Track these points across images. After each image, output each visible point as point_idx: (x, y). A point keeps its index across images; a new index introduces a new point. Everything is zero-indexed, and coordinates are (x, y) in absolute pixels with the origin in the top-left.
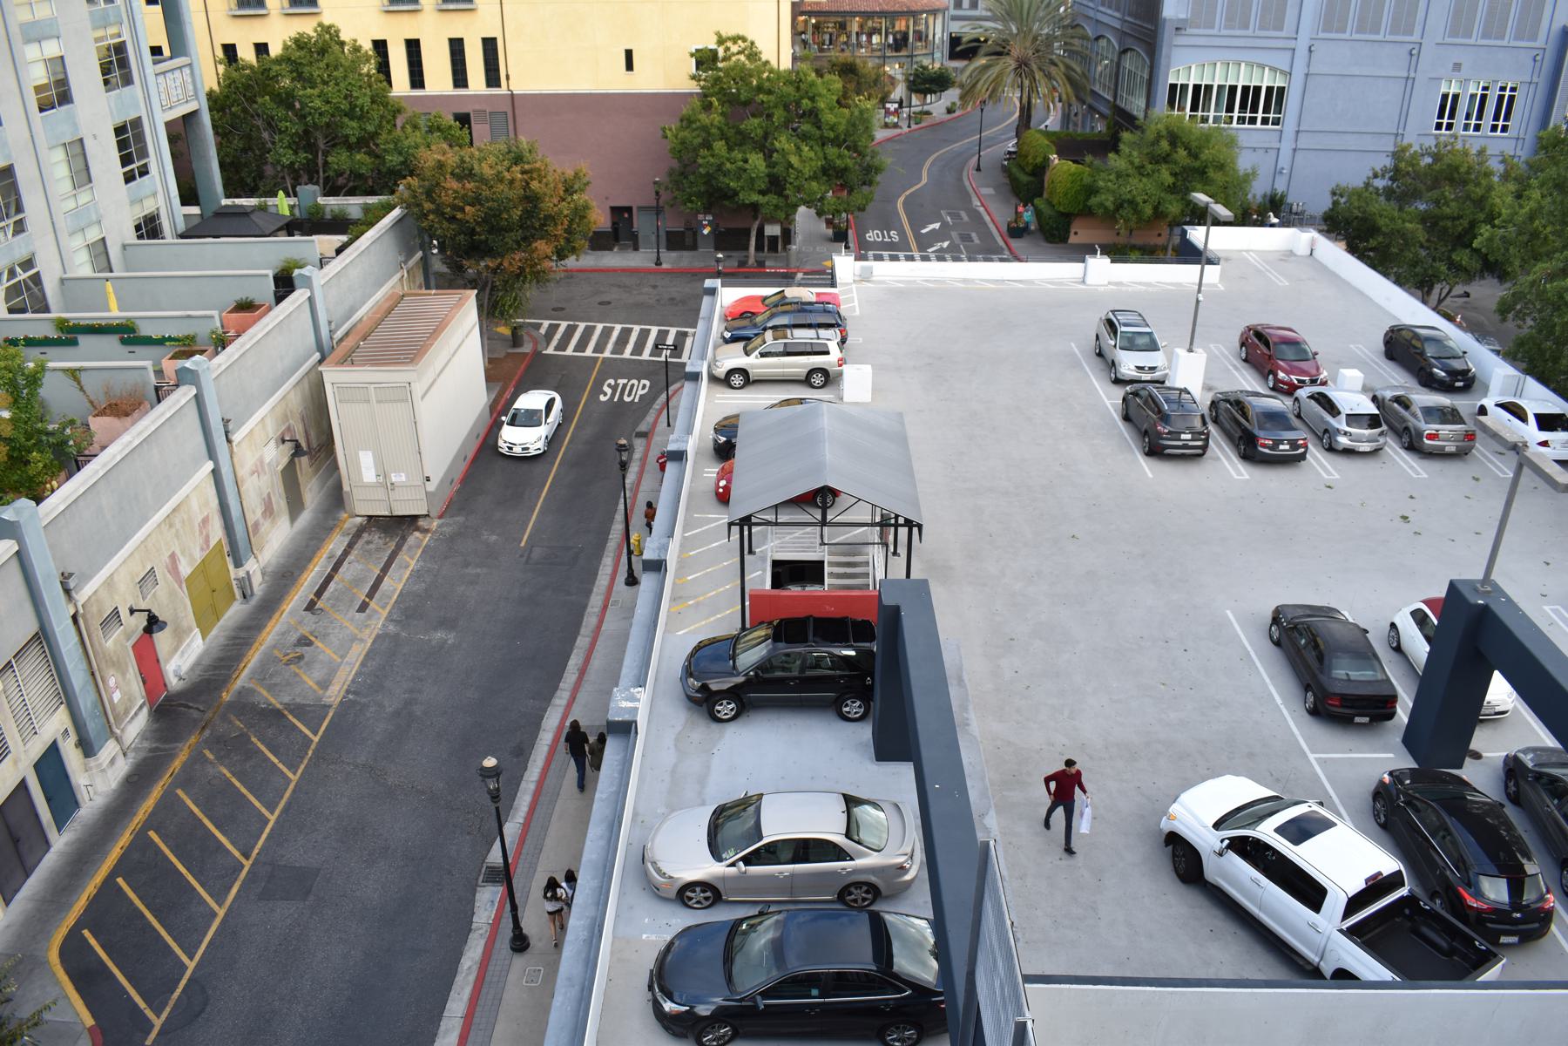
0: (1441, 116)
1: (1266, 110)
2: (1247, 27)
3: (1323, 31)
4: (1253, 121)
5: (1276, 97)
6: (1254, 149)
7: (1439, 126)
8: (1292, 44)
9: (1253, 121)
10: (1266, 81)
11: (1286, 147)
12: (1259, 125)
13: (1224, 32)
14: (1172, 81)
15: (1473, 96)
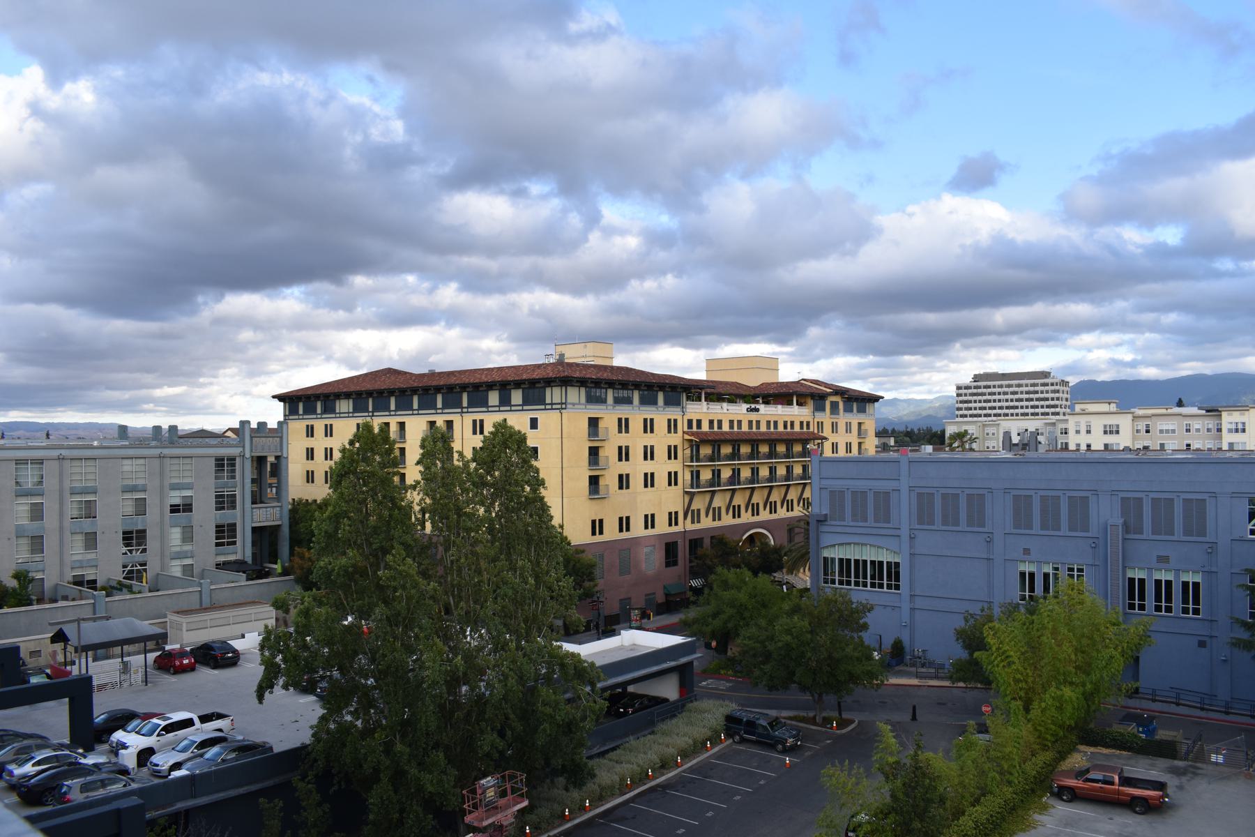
0: (1132, 597)
1: (857, 576)
2: (866, 521)
3: (943, 525)
4: (865, 585)
5: (894, 571)
6: (885, 606)
7: (1132, 607)
8: (897, 532)
9: (849, 583)
10: (885, 557)
11: (906, 607)
12: (885, 590)
13: (851, 524)
14: (825, 555)
15: (1046, 576)
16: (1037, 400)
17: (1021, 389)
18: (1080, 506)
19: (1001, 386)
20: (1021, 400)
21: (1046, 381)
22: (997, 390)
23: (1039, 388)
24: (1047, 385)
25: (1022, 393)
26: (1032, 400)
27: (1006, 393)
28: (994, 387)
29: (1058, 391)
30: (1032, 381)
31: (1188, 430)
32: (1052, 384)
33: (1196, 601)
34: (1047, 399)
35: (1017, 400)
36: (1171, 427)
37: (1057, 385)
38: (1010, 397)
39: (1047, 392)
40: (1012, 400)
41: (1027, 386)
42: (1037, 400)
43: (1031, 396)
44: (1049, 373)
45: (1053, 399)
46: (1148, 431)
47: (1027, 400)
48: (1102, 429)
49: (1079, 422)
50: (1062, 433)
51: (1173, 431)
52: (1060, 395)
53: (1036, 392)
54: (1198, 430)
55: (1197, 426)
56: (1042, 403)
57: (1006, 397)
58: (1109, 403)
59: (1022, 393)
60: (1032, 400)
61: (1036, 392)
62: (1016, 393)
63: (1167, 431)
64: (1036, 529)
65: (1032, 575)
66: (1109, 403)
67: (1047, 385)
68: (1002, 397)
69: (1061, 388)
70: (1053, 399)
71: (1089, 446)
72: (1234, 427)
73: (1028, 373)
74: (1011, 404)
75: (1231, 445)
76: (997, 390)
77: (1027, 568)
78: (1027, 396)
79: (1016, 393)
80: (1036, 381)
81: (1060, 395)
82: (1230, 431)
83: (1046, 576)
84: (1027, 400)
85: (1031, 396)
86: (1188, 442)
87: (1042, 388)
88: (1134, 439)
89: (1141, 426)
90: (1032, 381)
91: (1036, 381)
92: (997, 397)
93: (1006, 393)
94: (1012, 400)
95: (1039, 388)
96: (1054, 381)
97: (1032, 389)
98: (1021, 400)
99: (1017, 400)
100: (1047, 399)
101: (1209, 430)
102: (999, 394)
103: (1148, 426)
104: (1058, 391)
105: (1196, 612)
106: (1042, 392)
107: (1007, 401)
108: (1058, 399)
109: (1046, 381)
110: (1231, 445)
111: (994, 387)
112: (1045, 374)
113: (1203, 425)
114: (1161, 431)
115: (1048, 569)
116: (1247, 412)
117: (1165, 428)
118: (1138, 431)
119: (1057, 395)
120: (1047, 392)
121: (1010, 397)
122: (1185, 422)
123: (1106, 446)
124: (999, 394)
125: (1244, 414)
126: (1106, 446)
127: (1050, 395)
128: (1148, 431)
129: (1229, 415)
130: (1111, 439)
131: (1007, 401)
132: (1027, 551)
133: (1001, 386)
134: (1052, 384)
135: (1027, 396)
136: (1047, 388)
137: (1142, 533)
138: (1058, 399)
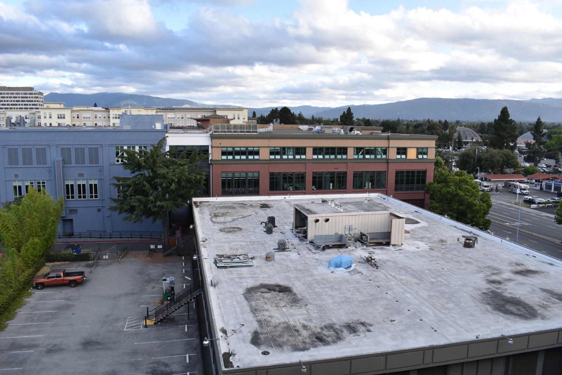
0: (68, 193)
15: (27, 187)
16: (27, 101)
17: (19, 96)
18: (42, 153)
19: (8, 94)
20: (19, 101)
21: (31, 92)
22: (6, 96)
23: (28, 96)
24: (32, 94)
25: (19, 97)
26: (24, 101)
27: (10, 97)
28: (4, 94)
29: (38, 98)
30: (24, 92)
31: (96, 117)
32: (35, 94)
33: (96, 192)
34: (32, 101)
35: (17, 101)
36: (88, 116)
37: (37, 94)
38: (13, 99)
39: (32, 98)
40: (14, 101)
41: (22, 94)
42: (27, 101)
43: (24, 99)
44: (33, 88)
45: (35, 101)
46: (78, 118)
47: (22, 101)
48: (57, 116)
49: (46, 113)
50: (38, 118)
51: (89, 118)
52: (39, 99)
53: (27, 98)
54: (100, 117)
55: (100, 116)
56: (30, 103)
57: (11, 99)
58: (60, 104)
59: (19, 97)
60: (24, 101)
61: (27, 98)
62: (16, 97)
63: (87, 118)
64: (21, 164)
65: (20, 187)
66: (60, 104)
67: (32, 94)
68: (8, 99)
69: (39, 96)
70: (35, 101)
71: (51, 124)
72: (115, 116)
73: (22, 88)
74: (14, 103)
75: (114, 124)
76: (6, 96)
77: (17, 184)
78: (22, 99)
79: (16, 97)
80: (26, 92)
81: (39, 99)
82: (113, 118)
83: (27, 187)
84: (22, 101)
85: (24, 99)
86: (96, 123)
87: (30, 96)
88: (72, 121)
89: (75, 115)
90: (24, 92)
91: (26, 92)
92: (6, 99)
93: (10, 97)
94: (14, 101)
95: (28, 96)
96: (36, 92)
97: (24, 96)
98: (19, 101)
99: (17, 101)
100: (32, 101)
101: (104, 117)
102: (7, 97)
103: (78, 115)
104: (38, 98)
105: (96, 197)
106: (30, 98)
107: (11, 101)
108: (38, 101)
109: (31, 92)
110: (114, 124)
111: (4, 94)
112: (31, 89)
113: (102, 115)
114: (84, 118)
115: (28, 183)
116: (120, 110)
117: (86, 116)
118: (74, 117)
119: (37, 99)
120: (32, 98)
121: (13, 99)
122: (94, 114)
123: (59, 124)
124: (7, 97)
125: (119, 111)
126: (59, 124)
127: (34, 99)
128: (78, 118)
129: (113, 111)
130: (61, 121)
131: (11, 101)
132: (16, 176)
133: (8, 94)
134: (35, 94)
135: (22, 99)
136: (32, 96)
137: (71, 164)
138: (38, 101)
